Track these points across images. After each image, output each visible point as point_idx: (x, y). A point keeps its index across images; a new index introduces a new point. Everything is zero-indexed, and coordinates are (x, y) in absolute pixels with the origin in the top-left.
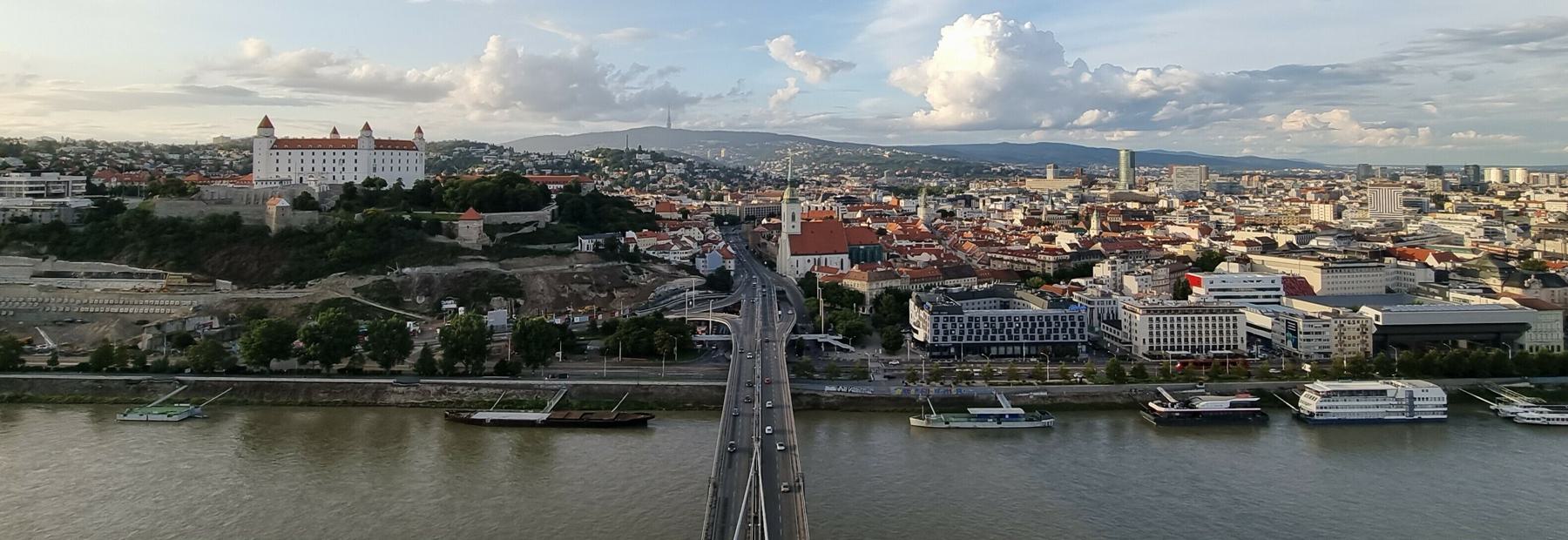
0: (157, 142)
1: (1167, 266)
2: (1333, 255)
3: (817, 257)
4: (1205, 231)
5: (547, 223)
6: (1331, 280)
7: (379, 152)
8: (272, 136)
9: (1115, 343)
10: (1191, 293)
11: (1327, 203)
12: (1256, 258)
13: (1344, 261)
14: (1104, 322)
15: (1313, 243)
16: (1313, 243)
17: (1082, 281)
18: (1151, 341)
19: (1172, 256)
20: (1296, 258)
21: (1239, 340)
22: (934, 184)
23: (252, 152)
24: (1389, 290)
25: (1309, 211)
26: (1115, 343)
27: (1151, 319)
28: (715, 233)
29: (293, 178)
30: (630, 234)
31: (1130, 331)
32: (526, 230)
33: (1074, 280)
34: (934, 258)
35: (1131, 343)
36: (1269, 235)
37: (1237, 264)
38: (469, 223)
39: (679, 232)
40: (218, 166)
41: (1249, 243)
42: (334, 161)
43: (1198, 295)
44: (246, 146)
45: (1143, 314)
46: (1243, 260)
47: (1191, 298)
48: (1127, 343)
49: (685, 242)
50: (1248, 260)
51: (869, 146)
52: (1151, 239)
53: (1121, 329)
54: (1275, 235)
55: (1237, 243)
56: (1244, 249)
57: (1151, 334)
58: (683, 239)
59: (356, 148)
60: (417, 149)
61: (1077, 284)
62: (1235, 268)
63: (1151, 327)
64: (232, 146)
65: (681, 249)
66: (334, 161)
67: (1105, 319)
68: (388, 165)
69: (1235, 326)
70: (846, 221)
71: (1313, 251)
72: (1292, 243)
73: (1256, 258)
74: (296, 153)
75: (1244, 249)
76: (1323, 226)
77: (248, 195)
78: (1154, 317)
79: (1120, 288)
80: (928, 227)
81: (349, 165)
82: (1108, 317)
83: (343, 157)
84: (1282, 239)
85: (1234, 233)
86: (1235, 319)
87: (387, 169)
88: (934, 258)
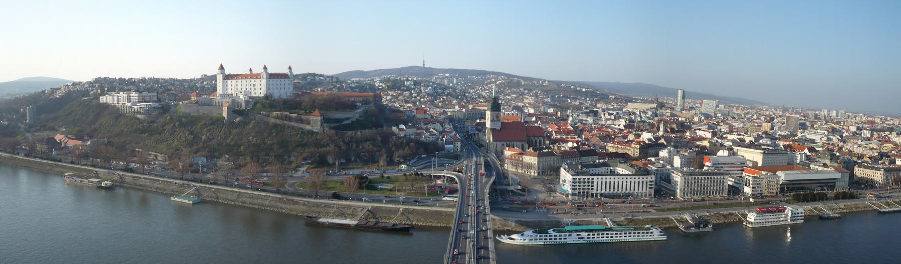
0: (180, 78)
1: (695, 151)
2: (768, 148)
3: (508, 143)
4: (714, 135)
5: (357, 119)
6: (766, 159)
7: (271, 80)
8: (224, 73)
9: (667, 191)
10: (704, 166)
11: (769, 123)
12: (736, 148)
13: (772, 151)
14: (663, 180)
15: (761, 142)
16: (761, 142)
17: (653, 159)
18: (684, 190)
19: (698, 147)
20: (753, 149)
21: (724, 188)
22: (577, 103)
23: (216, 81)
24: (789, 164)
25: (761, 126)
26: (667, 191)
27: (685, 179)
28: (448, 127)
29: (233, 93)
30: (403, 127)
31: (675, 185)
32: (346, 122)
33: (649, 159)
34: (575, 145)
35: (675, 191)
36: (743, 137)
37: (727, 152)
38: (316, 118)
39: (429, 126)
40: (203, 88)
41: (733, 141)
42: (251, 85)
43: (708, 166)
44: (214, 78)
45: (682, 176)
46: (730, 149)
47: (705, 168)
48: (673, 191)
49: (432, 132)
50: (732, 150)
51: (541, 80)
52: (689, 138)
53: (670, 184)
54: (745, 137)
55: (729, 141)
56: (731, 144)
57: (684, 186)
58: (432, 130)
59: (260, 78)
60: (289, 78)
61: (651, 161)
62: (726, 153)
63: (685, 182)
64: (205, 78)
65: (430, 136)
66: (251, 85)
67: (663, 179)
68: (275, 87)
69: (723, 182)
70: (526, 122)
71: (760, 145)
72: (752, 141)
73: (736, 148)
74: (234, 81)
75: (731, 144)
76: (766, 133)
77: (222, 102)
78: (687, 178)
79: (671, 163)
80: (572, 127)
81: (258, 87)
82: (665, 178)
83: (255, 83)
84: (748, 139)
85: (727, 136)
86: (724, 178)
87: (275, 89)
88: (575, 145)
